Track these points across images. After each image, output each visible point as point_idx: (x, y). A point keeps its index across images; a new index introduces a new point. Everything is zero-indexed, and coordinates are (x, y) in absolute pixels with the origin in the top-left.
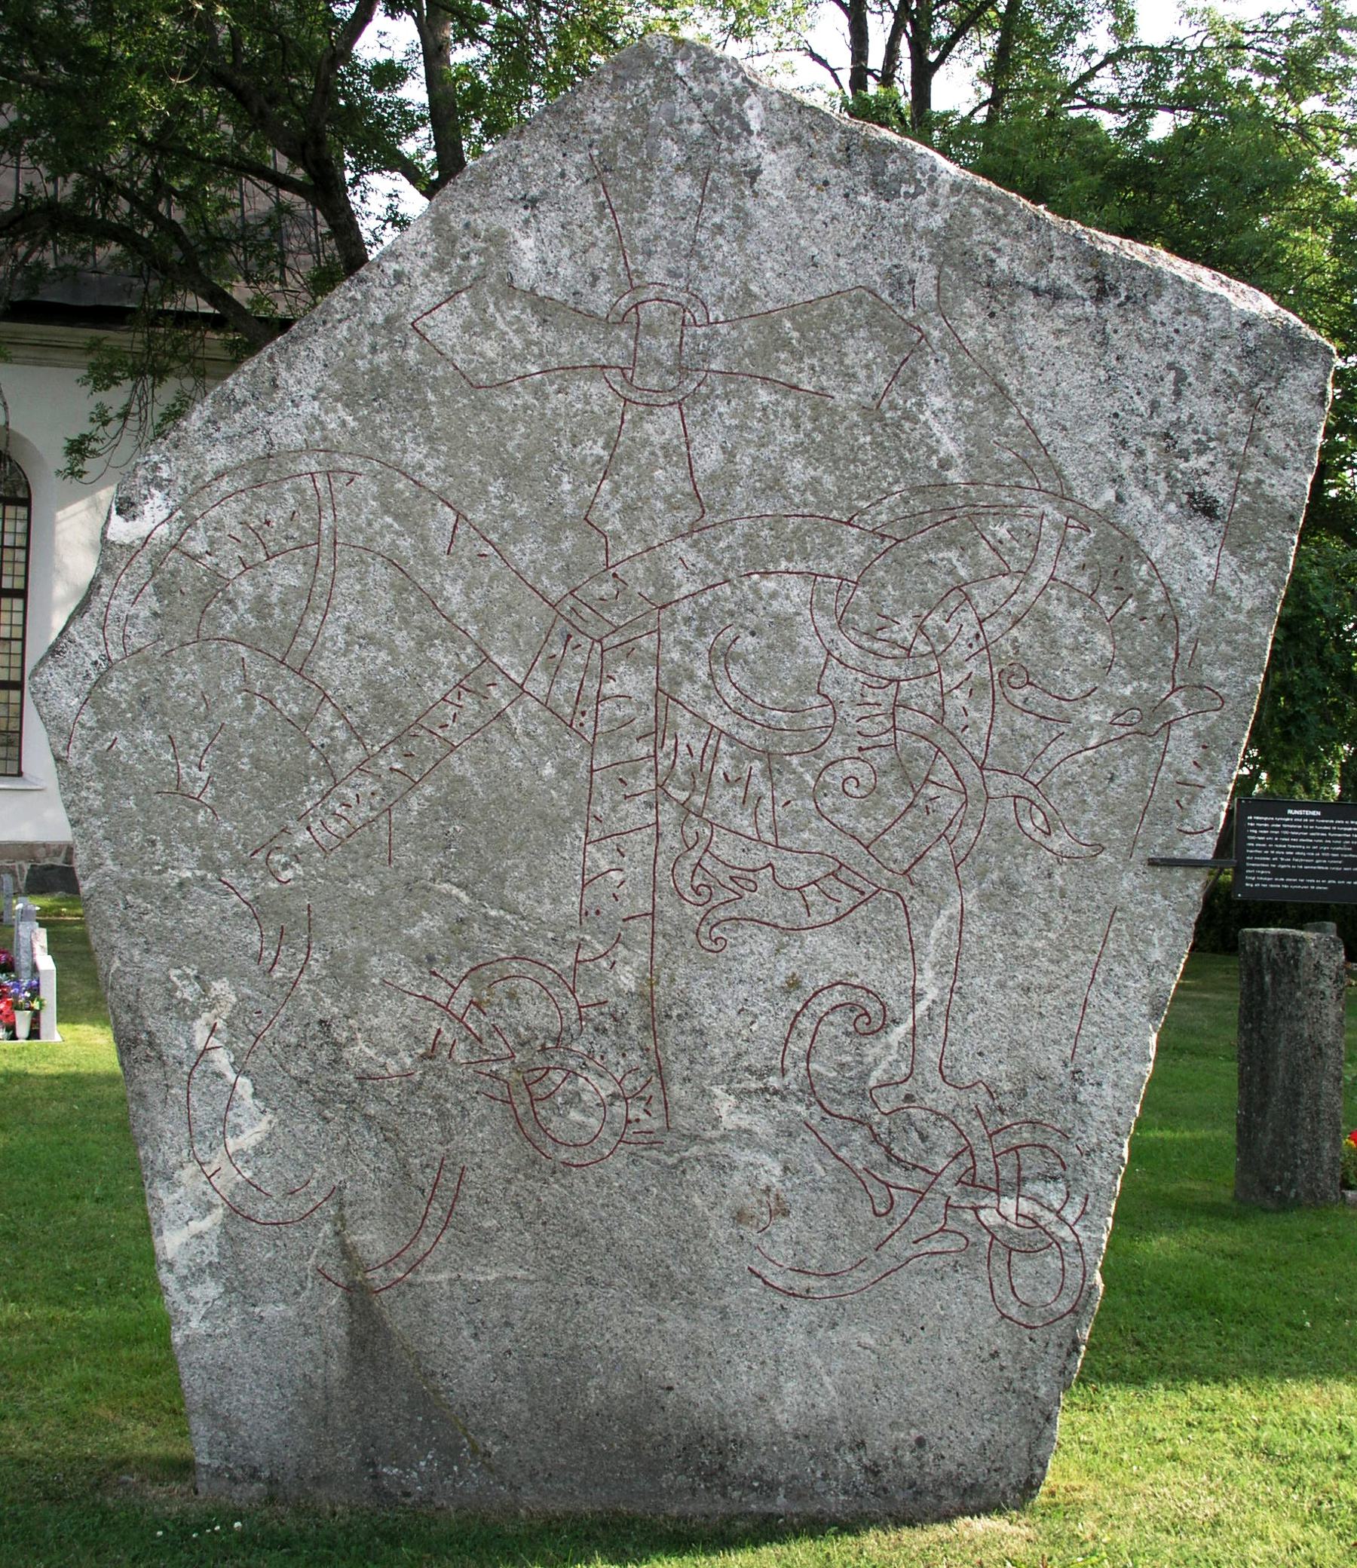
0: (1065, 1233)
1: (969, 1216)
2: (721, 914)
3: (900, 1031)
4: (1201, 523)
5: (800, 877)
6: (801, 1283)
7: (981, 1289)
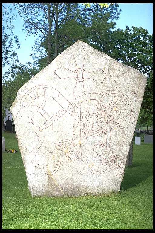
0: (121, 166)
1: (112, 165)
2: (87, 135)
3: (105, 147)
4: (134, 95)
5: (95, 131)
6: (95, 172)
7: (113, 172)
